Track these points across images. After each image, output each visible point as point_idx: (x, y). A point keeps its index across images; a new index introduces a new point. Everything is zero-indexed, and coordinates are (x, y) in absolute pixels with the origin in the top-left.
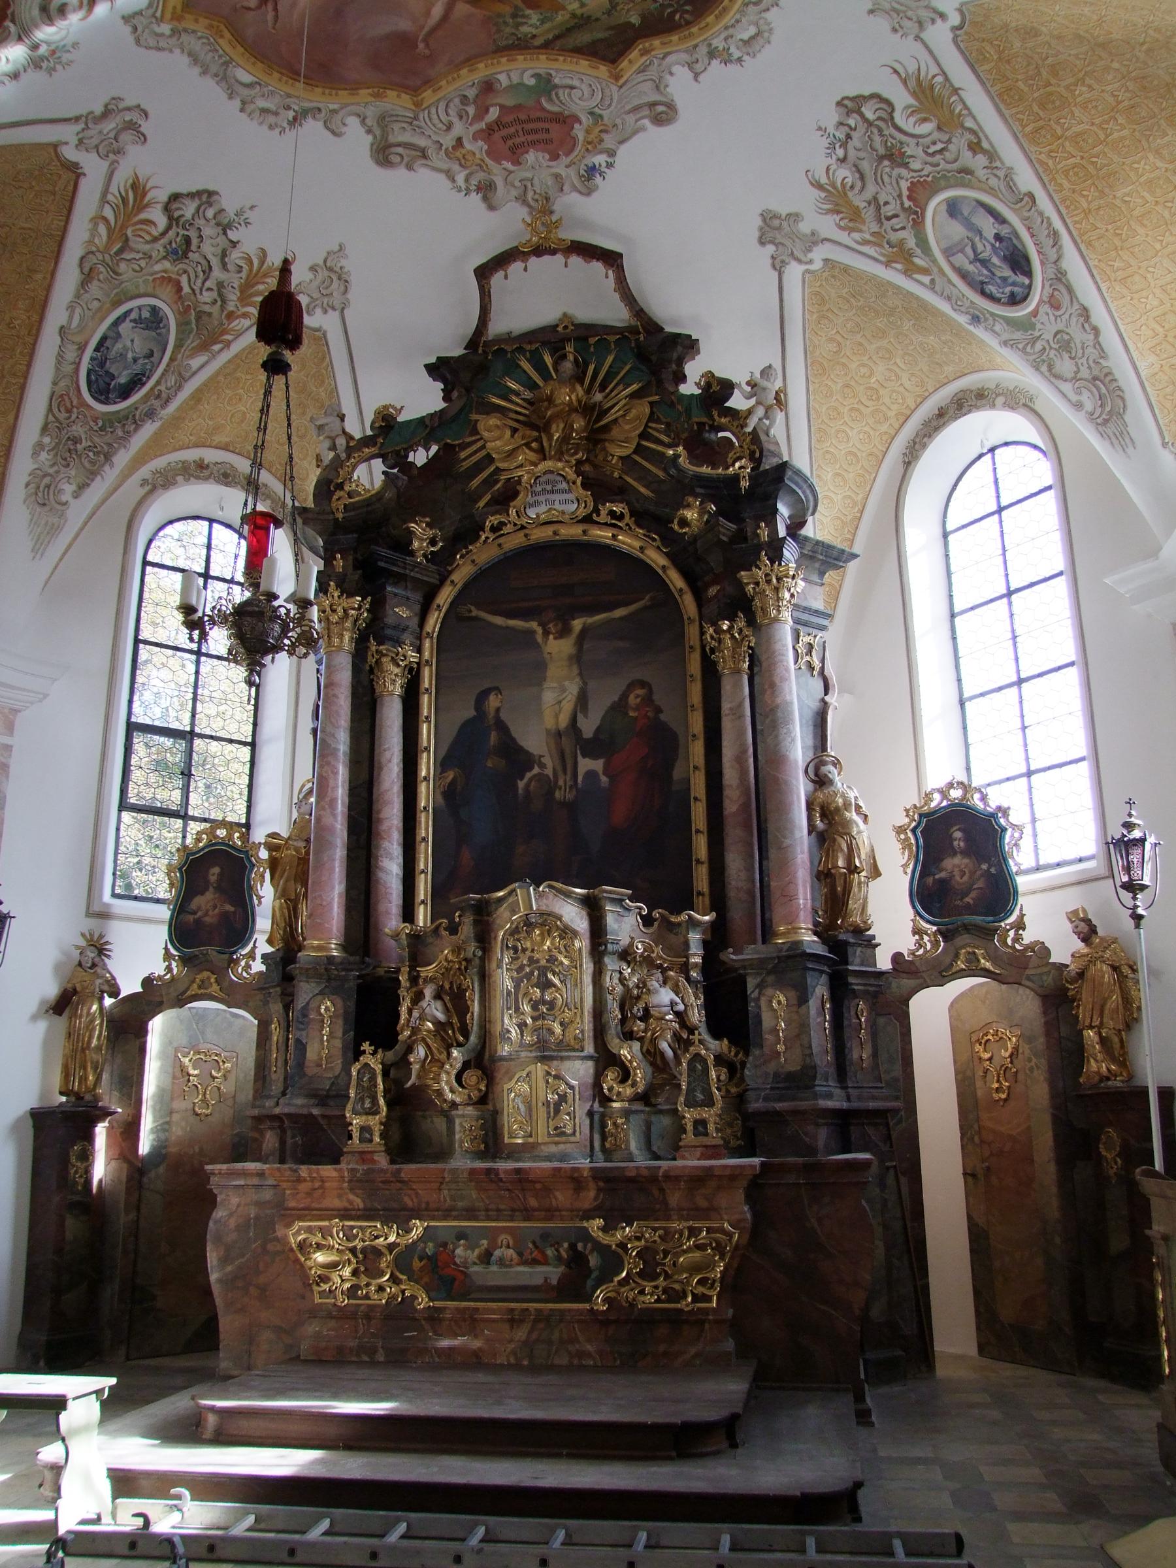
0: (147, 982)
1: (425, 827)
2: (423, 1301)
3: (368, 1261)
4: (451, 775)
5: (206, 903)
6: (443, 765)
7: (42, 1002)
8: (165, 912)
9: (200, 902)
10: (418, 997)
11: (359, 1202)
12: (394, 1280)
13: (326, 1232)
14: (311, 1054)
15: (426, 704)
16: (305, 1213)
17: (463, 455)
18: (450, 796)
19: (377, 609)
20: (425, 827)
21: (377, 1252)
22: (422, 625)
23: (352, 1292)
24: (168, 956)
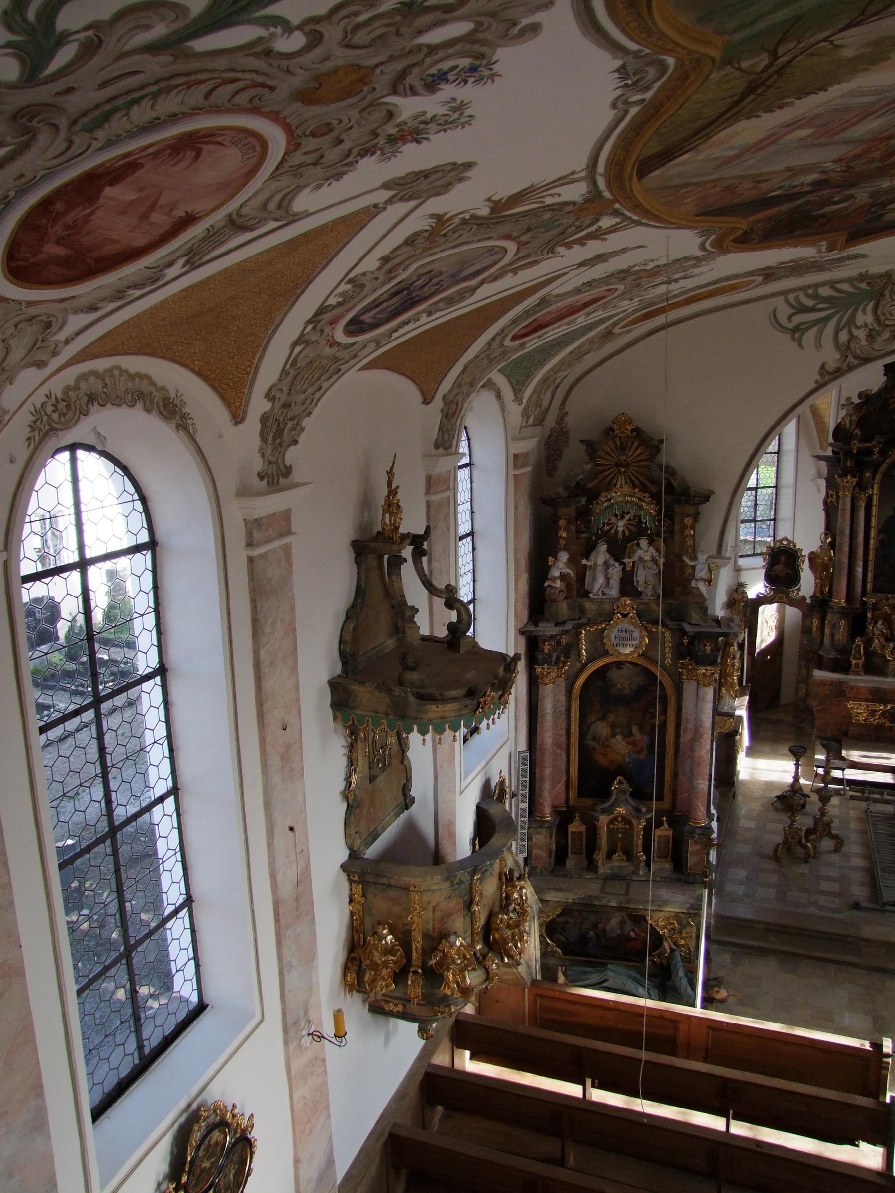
0: (758, 595)
1: (871, 557)
2: (887, 724)
3: (872, 713)
4: (882, 536)
5: (779, 568)
6: (880, 532)
7: (724, 604)
8: (763, 571)
9: (776, 567)
10: (876, 622)
11: (870, 697)
12: (879, 718)
13: (860, 705)
14: (836, 637)
15: (874, 510)
16: (855, 699)
17: (891, 402)
18: (882, 545)
19: (861, 477)
20: (871, 557)
21: (876, 711)
22: (873, 478)
23: (865, 720)
24: (766, 587)
